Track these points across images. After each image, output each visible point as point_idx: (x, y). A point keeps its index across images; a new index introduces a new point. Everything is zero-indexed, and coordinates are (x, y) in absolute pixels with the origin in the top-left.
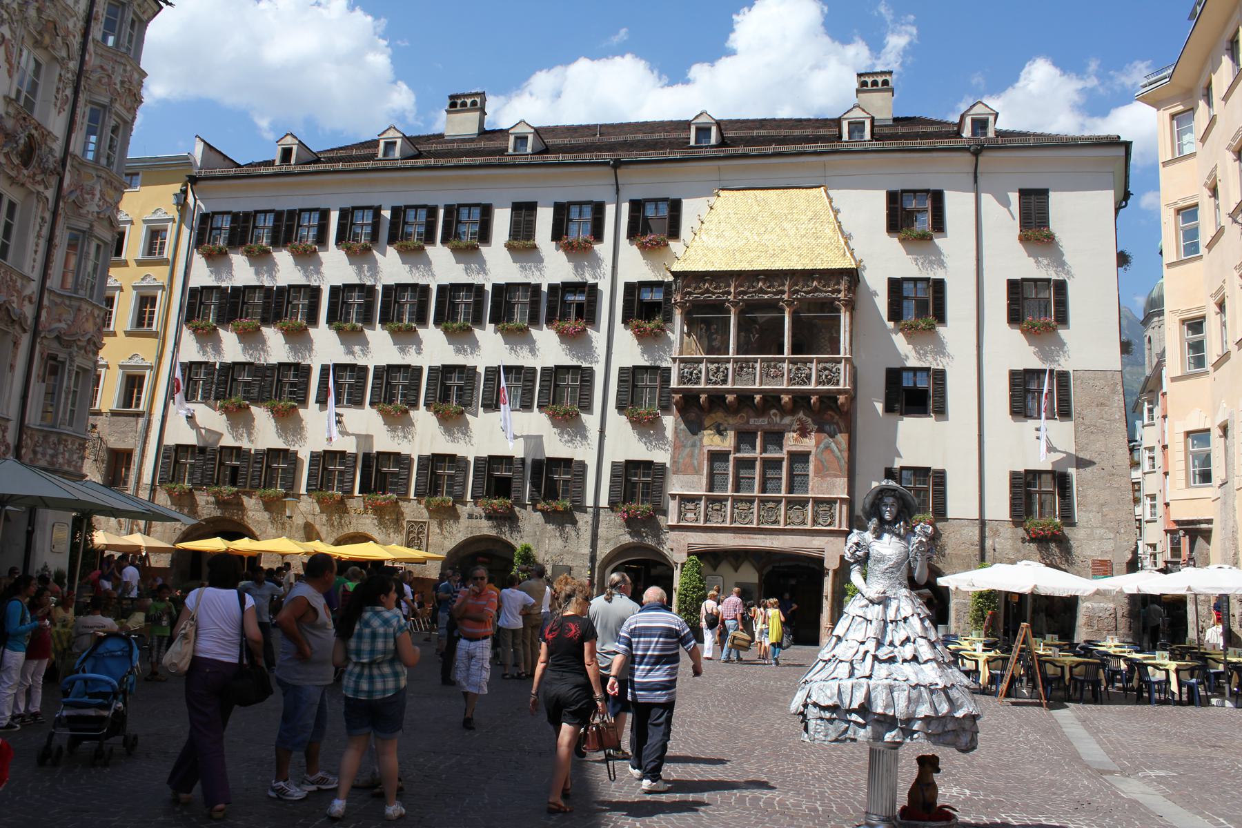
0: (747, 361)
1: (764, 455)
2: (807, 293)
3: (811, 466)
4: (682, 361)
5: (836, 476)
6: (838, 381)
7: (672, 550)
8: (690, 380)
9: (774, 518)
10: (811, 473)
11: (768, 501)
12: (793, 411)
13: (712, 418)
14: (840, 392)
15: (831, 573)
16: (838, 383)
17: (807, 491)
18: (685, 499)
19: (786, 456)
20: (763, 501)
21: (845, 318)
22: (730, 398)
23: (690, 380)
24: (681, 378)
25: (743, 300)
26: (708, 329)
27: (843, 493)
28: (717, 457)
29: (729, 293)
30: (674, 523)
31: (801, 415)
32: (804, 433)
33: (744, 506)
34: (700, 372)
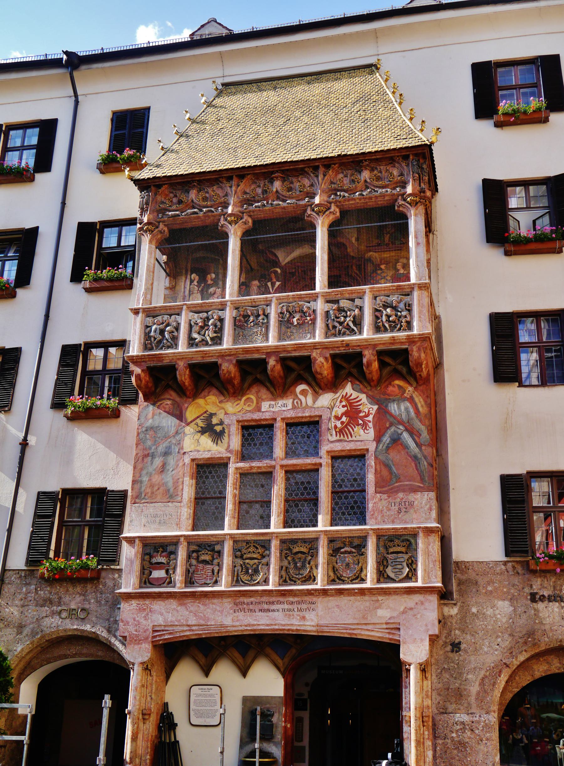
1: (285, 462)
3: (371, 478)
5: (414, 490)
7: (125, 638)
8: (160, 341)
10: (371, 488)
13: (199, 406)
14: (411, 340)
16: (409, 326)
17: (363, 522)
19: (325, 460)
26: (203, 279)
27: (427, 520)
29: (225, 205)
30: (129, 590)
31: (348, 389)
34: (177, 329)
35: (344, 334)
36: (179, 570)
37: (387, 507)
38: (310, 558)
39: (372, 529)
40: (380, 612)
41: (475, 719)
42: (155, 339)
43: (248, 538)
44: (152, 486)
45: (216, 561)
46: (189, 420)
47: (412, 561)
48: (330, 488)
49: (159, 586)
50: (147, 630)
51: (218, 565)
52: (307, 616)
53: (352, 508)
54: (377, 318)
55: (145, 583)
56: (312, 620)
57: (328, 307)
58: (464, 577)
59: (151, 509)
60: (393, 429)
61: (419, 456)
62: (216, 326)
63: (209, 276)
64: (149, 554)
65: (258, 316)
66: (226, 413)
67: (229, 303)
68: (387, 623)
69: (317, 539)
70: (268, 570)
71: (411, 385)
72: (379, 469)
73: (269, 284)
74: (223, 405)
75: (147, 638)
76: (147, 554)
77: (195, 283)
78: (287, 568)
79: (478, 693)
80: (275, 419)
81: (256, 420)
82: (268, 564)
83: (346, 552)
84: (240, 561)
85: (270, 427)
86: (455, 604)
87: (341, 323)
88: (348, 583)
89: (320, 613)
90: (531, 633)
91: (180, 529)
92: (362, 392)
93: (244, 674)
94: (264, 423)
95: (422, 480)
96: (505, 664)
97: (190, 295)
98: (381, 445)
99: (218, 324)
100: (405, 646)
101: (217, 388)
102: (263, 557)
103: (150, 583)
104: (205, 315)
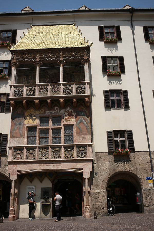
0: (44, 85)
2: (70, 57)
4: (14, 86)
5: (86, 135)
6: (85, 92)
8: (18, 94)
9: (58, 156)
10: (75, 134)
11: (55, 148)
12: (65, 107)
15: (87, 181)
16: (85, 93)
18: (16, 149)
19: (63, 127)
20: (53, 148)
21: (86, 67)
22: (37, 101)
23: (18, 94)
24: (15, 94)
25: (41, 61)
28: (31, 129)
29: (36, 59)
31: (69, 108)
32: (70, 115)
33: (44, 151)
34: (23, 91)
35: (68, 94)
36: (24, 155)
37: (79, 139)
38: (59, 152)
39: (75, 145)
40: (78, 165)
41: (101, 191)
42: (17, 94)
43: (43, 147)
44: (16, 133)
45: (34, 153)
46: (26, 116)
47: (86, 153)
48: (64, 134)
49: (19, 160)
50: (16, 171)
51: (35, 154)
52: (59, 167)
53: (70, 139)
54: (77, 90)
55: (15, 159)
56: (60, 168)
57: (63, 87)
58: (98, 156)
59: (16, 139)
60: (80, 119)
61: (87, 126)
62: (33, 90)
63: (29, 77)
64: (16, 151)
65: (45, 88)
66: (36, 114)
67: (37, 85)
68: (79, 168)
69: (61, 147)
70: (48, 155)
71: (85, 108)
72: (77, 129)
73: (46, 80)
74: (35, 112)
75: (16, 174)
76: (15, 151)
77: (26, 79)
78: (53, 155)
79: (102, 185)
80: (49, 116)
81: (44, 116)
82: (48, 154)
83: (69, 150)
84: (41, 153)
85: (49, 117)
86: (96, 163)
87: (67, 91)
88: (69, 158)
89: (62, 166)
90: (114, 170)
91: (24, 144)
92: (72, 109)
93: (41, 182)
94: (46, 117)
95: (88, 132)
96: (108, 177)
97: (24, 82)
98: (77, 123)
99: (34, 90)
100: (84, 174)
101: (34, 107)
102: (47, 152)
103: (16, 159)
104: (30, 88)
